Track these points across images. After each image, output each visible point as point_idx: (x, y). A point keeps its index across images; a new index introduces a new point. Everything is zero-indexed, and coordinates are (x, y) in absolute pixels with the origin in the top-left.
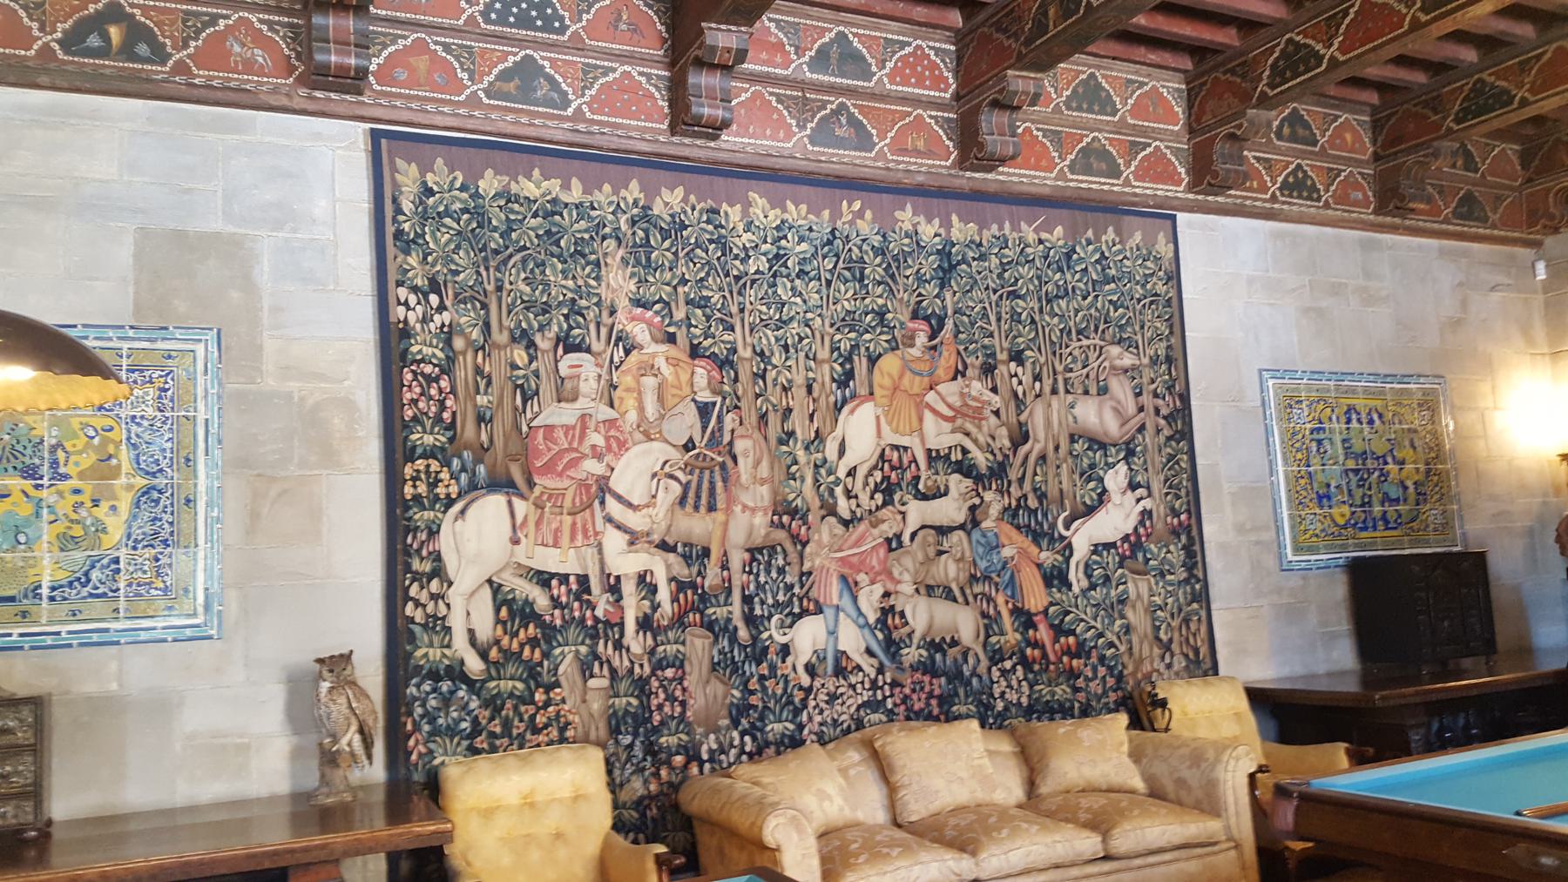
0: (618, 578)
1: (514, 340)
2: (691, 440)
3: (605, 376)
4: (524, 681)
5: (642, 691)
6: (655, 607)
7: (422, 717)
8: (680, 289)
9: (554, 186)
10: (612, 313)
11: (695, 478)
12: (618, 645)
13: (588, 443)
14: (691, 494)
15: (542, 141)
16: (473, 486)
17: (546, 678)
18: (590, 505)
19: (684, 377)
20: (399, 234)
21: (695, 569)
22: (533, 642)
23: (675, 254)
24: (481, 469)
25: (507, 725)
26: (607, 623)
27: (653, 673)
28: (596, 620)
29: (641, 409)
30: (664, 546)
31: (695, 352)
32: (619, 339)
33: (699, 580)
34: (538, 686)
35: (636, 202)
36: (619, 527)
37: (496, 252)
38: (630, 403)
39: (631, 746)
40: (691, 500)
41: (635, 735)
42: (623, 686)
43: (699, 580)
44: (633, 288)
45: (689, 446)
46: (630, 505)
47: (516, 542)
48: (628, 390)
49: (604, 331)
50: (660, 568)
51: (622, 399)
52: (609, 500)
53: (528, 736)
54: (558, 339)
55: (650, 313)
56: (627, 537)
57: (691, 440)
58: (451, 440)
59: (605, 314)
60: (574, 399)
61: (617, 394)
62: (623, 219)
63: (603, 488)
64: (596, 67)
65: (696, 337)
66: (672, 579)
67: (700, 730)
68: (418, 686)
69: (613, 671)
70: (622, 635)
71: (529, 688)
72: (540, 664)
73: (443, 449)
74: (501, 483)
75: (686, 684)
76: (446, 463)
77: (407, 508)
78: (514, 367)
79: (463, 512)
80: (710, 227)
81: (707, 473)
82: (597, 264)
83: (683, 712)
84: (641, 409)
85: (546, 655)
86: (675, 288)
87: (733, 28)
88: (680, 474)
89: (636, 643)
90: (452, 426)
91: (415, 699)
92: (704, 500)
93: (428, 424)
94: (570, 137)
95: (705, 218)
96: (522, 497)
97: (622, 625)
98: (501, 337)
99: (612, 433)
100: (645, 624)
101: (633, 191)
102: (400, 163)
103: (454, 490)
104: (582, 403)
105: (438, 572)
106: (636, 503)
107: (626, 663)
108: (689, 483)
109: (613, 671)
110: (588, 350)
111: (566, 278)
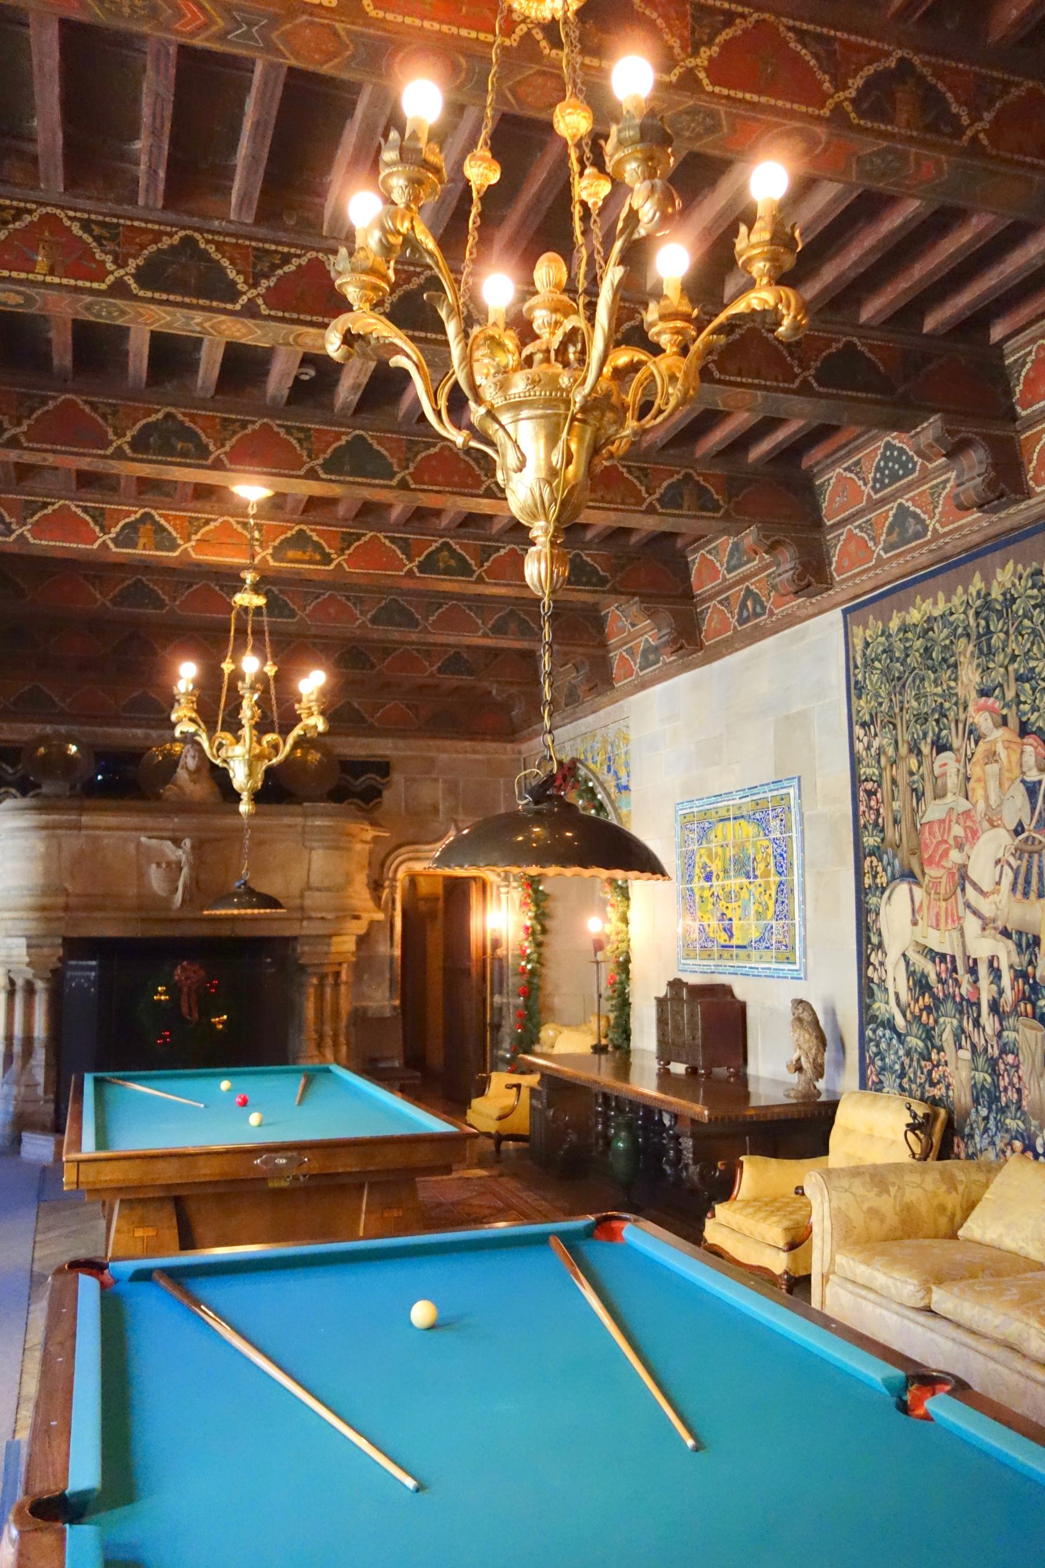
0: (975, 961)
1: (911, 751)
2: (1020, 824)
3: (962, 770)
4: (923, 1041)
5: (994, 1070)
6: (1001, 992)
7: (876, 1055)
8: (1011, 668)
9: (927, 606)
10: (965, 708)
11: (1025, 863)
12: (977, 1023)
13: (952, 834)
14: (1021, 880)
15: (917, 571)
16: (894, 878)
17: (937, 1042)
18: (955, 893)
19: (1015, 757)
20: (857, 682)
21: (1027, 958)
22: (928, 1009)
23: (1007, 633)
24: (897, 862)
25: (915, 1073)
26: (970, 1004)
27: (1000, 1057)
28: (962, 998)
29: (987, 798)
30: (1006, 933)
31: (1024, 730)
32: (971, 732)
33: (1030, 969)
34: (933, 1046)
35: (978, 593)
36: (976, 913)
37: (899, 679)
38: (980, 792)
39: (986, 1119)
40: (1020, 887)
41: (990, 1109)
42: (981, 1061)
43: (1030, 969)
44: (978, 680)
45: (1019, 830)
46: (981, 892)
47: (915, 923)
48: (979, 780)
49: (961, 726)
50: (1006, 954)
51: (973, 789)
52: (969, 888)
53: (927, 1087)
54: (933, 743)
55: (992, 700)
56: (980, 922)
57: (1020, 824)
58: (883, 840)
59: (961, 710)
60: (944, 795)
61: (972, 784)
62: (971, 613)
63: (962, 877)
64: (937, 486)
65: (1025, 714)
66: (1011, 967)
67: (1034, 1122)
68: (874, 1031)
69: (974, 1046)
70: (979, 1015)
71: (926, 1046)
72: (933, 1029)
73: (878, 848)
74: (909, 875)
75: (1021, 1073)
76: (880, 860)
77: (866, 894)
78: (911, 774)
79: (889, 898)
80: (1035, 592)
81: (1036, 856)
82: (955, 666)
83: (1020, 1100)
84: (987, 798)
85: (936, 1021)
86: (1006, 668)
87: (925, 425)
88: (1012, 860)
89: (988, 1021)
90: (882, 831)
91: (871, 1040)
92: (1020, 887)
93: (870, 828)
94: (931, 557)
95: (1030, 584)
96: (919, 884)
97: (978, 1005)
98: (903, 750)
99: (969, 823)
100: (995, 1007)
101: (977, 584)
102: (855, 628)
103: (884, 880)
104: (950, 798)
105: (880, 945)
106: (985, 890)
107: (983, 1042)
108: (1019, 867)
109: (974, 1046)
110: (950, 749)
111: (936, 686)
